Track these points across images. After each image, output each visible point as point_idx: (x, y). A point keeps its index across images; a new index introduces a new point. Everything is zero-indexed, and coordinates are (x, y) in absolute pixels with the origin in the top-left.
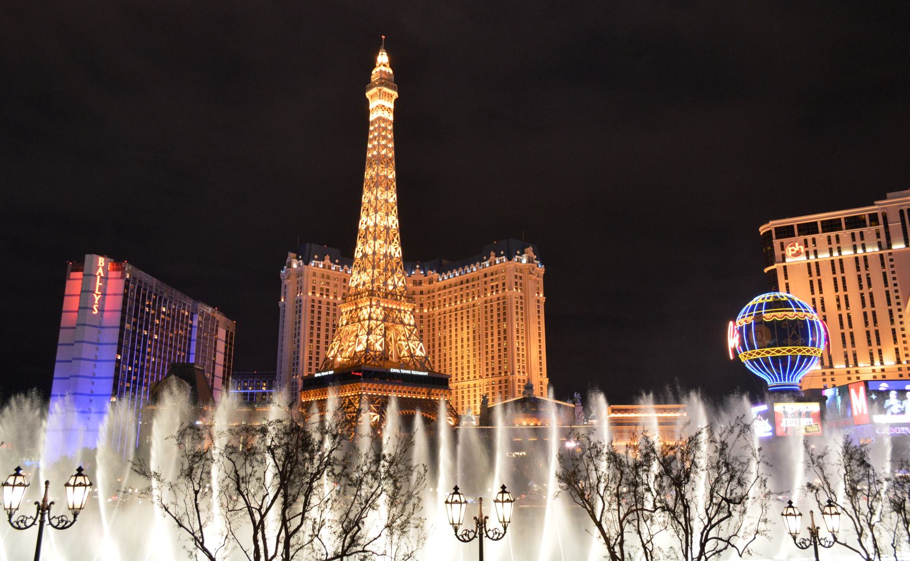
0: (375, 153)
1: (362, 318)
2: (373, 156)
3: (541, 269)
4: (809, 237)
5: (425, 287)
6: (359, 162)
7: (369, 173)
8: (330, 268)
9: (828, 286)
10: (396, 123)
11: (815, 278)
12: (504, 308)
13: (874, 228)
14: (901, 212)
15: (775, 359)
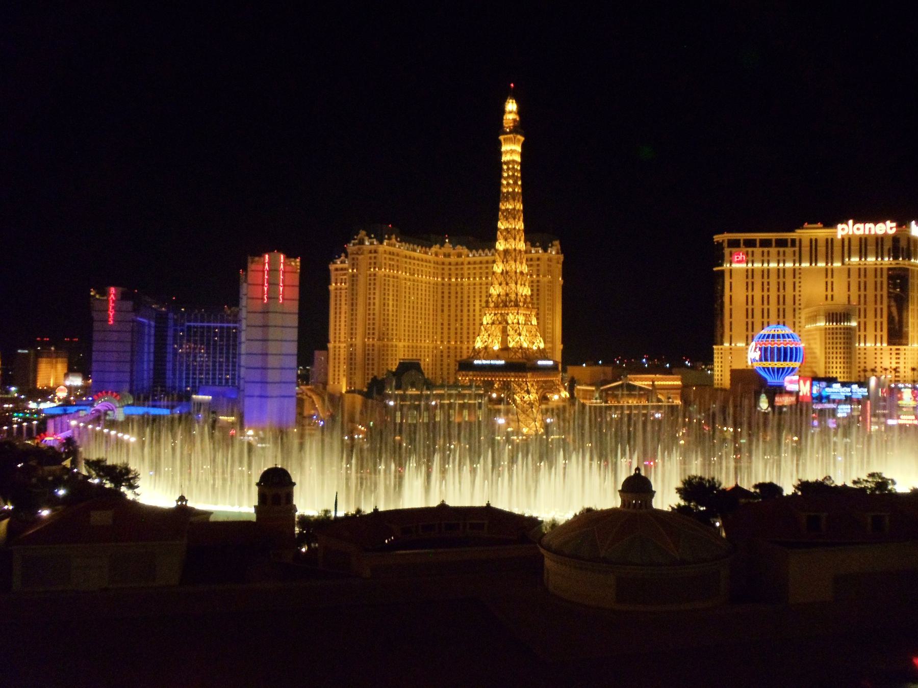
0: (510, 190)
1: (510, 322)
2: (508, 192)
3: (561, 257)
4: (750, 250)
5: (453, 259)
6: (494, 195)
7: (505, 206)
8: (395, 246)
9: (758, 287)
10: (522, 164)
11: (750, 280)
12: (538, 290)
13: (793, 249)
14: (811, 240)
15: (778, 369)
